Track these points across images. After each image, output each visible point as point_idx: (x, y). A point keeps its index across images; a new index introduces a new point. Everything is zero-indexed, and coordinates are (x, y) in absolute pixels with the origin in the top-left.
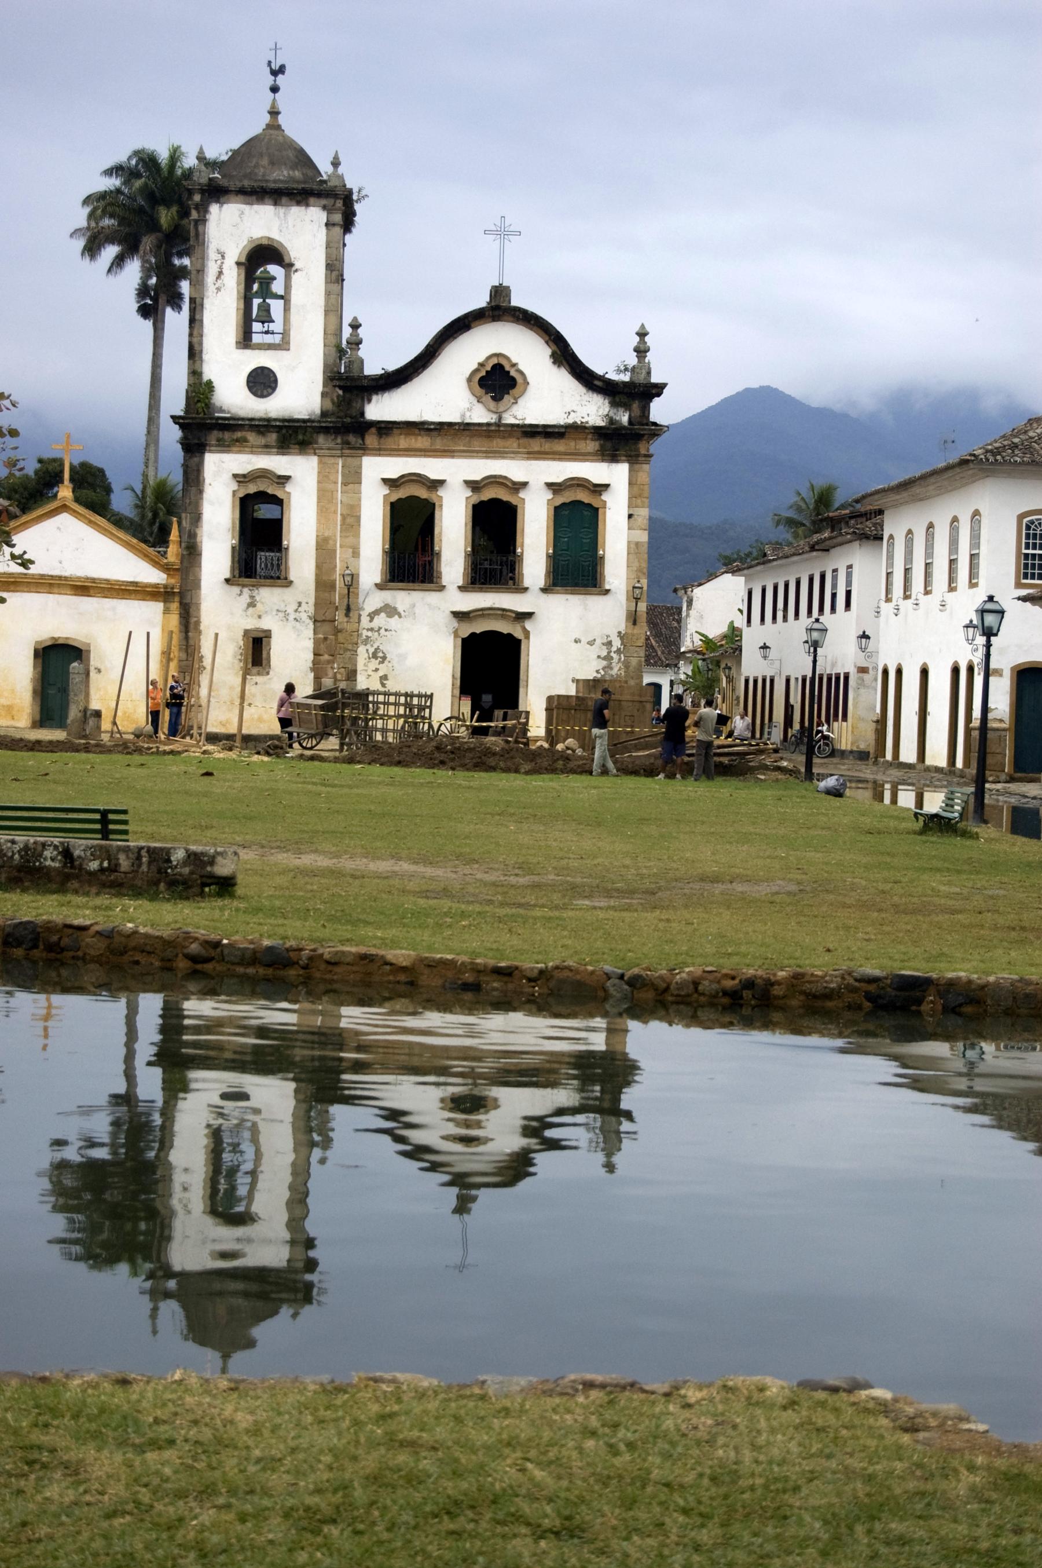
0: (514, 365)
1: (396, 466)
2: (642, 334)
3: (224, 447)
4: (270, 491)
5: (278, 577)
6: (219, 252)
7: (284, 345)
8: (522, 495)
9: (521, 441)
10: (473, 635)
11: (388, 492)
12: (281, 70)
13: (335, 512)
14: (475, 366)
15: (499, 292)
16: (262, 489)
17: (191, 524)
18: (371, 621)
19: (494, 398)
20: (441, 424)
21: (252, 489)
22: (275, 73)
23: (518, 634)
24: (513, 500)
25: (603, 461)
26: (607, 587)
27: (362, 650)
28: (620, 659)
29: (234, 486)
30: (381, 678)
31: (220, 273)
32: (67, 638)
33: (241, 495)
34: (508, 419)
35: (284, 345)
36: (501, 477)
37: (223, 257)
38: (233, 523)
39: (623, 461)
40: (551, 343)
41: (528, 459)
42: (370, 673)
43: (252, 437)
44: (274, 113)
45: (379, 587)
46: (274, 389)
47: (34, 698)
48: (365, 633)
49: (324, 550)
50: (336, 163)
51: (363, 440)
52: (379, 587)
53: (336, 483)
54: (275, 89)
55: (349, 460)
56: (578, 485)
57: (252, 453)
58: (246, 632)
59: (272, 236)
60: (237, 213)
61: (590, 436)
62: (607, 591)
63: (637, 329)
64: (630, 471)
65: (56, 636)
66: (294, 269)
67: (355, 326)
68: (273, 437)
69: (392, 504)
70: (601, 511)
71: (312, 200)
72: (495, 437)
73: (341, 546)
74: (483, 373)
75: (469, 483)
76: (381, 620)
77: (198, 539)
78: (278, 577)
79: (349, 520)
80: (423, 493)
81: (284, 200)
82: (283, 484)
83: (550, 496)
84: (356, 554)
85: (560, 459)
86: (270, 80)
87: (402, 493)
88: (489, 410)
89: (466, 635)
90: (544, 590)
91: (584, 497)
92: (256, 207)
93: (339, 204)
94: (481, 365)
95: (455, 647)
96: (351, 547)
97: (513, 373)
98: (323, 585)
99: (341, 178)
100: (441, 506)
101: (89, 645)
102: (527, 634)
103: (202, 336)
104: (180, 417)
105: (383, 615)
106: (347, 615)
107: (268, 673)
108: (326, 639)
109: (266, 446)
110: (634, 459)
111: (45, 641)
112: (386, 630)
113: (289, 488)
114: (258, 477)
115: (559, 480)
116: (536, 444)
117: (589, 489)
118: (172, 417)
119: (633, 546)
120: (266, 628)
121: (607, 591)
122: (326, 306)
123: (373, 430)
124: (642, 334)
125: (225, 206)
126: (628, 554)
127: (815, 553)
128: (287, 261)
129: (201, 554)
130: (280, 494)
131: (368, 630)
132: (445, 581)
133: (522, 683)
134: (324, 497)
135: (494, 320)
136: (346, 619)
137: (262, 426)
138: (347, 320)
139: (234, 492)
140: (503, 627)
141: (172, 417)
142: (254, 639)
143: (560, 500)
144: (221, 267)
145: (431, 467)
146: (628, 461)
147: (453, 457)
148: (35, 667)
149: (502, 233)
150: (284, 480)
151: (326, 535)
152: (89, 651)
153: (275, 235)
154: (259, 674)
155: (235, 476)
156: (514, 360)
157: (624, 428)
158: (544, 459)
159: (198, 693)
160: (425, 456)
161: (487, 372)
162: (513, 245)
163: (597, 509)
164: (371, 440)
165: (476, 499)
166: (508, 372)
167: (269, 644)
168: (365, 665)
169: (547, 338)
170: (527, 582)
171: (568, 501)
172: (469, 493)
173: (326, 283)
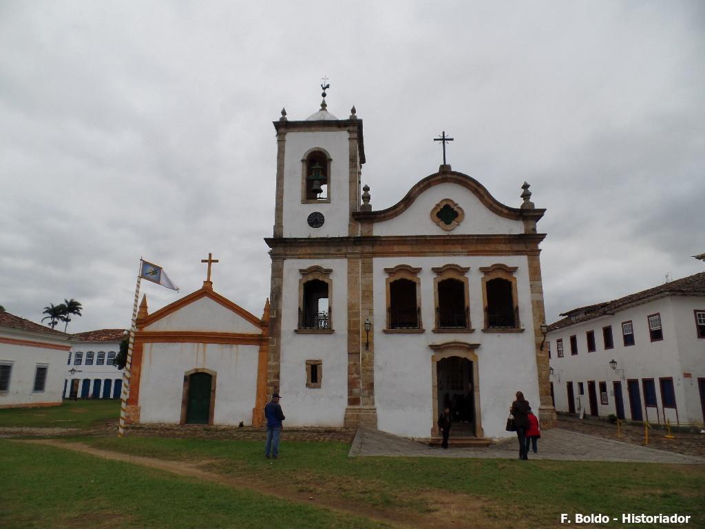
0: (456, 205)
1: (393, 262)
2: (526, 187)
4: (320, 279)
7: (328, 201)
8: (467, 275)
10: (443, 359)
11: (388, 277)
12: (328, 86)
13: (359, 289)
14: (434, 206)
15: (445, 169)
16: (316, 278)
21: (310, 278)
22: (324, 89)
23: (470, 357)
25: (512, 255)
26: (522, 328)
32: (204, 369)
33: (304, 281)
35: (328, 201)
36: (453, 265)
39: (524, 255)
41: (468, 255)
44: (324, 105)
45: (385, 332)
46: (322, 224)
47: (182, 406)
49: (352, 312)
50: (353, 111)
52: (385, 332)
53: (358, 273)
54: (324, 95)
55: (367, 260)
56: (500, 269)
57: (310, 258)
58: (307, 363)
59: (321, 146)
63: (522, 185)
67: (367, 189)
69: (391, 284)
70: (513, 284)
72: (447, 244)
73: (363, 309)
74: (439, 210)
77: (279, 308)
80: (409, 277)
82: (328, 274)
83: (483, 276)
84: (371, 311)
85: (487, 255)
86: (323, 91)
87: (397, 277)
88: (443, 229)
89: (439, 359)
90: (484, 331)
93: (356, 128)
94: (438, 205)
97: (456, 209)
98: (353, 332)
99: (356, 117)
101: (216, 373)
104: (269, 239)
108: (355, 364)
111: (191, 371)
114: (314, 271)
117: (506, 270)
118: (265, 239)
119: (535, 302)
122: (350, 179)
123: (378, 242)
124: (526, 187)
127: (606, 316)
128: (328, 157)
130: (326, 281)
132: (424, 327)
138: (362, 186)
139: (300, 281)
140: (461, 354)
141: (265, 239)
143: (489, 278)
145: (413, 262)
146: (526, 254)
147: (424, 256)
148: (184, 385)
149: (444, 139)
150: (329, 272)
151: (353, 302)
152: (215, 376)
154: (315, 387)
155: (301, 271)
156: (456, 202)
158: (478, 255)
160: (409, 256)
161: (441, 209)
162: (449, 144)
164: (377, 249)
165: (440, 279)
170: (473, 327)
171: (493, 278)
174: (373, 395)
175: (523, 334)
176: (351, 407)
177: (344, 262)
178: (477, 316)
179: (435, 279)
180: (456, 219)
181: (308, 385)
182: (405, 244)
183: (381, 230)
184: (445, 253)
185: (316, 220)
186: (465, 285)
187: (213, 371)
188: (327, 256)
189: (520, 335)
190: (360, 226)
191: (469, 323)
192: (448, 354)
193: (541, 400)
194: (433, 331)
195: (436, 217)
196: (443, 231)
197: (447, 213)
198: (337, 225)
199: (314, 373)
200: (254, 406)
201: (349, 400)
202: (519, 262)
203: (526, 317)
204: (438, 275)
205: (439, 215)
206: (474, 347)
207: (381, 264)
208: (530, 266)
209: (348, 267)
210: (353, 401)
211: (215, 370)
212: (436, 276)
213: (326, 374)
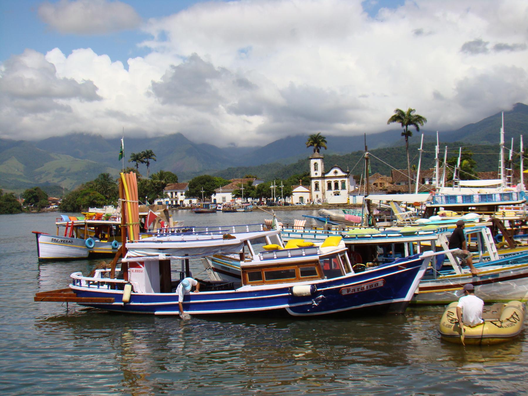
5: (319, 190)
34: (337, 175)
45: (327, 190)
49: (322, 187)
52: (327, 190)
78: (319, 190)
84: (325, 187)
90: (341, 190)
98: (322, 190)
110: (348, 178)
134: (322, 183)
150: (318, 182)
177: (321, 180)
183: (326, 176)
185: (316, 174)
188: (318, 179)
197: (336, 172)
198: (319, 175)
199: (317, 196)
202: (346, 179)
203: (347, 187)
206: (339, 192)
207: (326, 180)
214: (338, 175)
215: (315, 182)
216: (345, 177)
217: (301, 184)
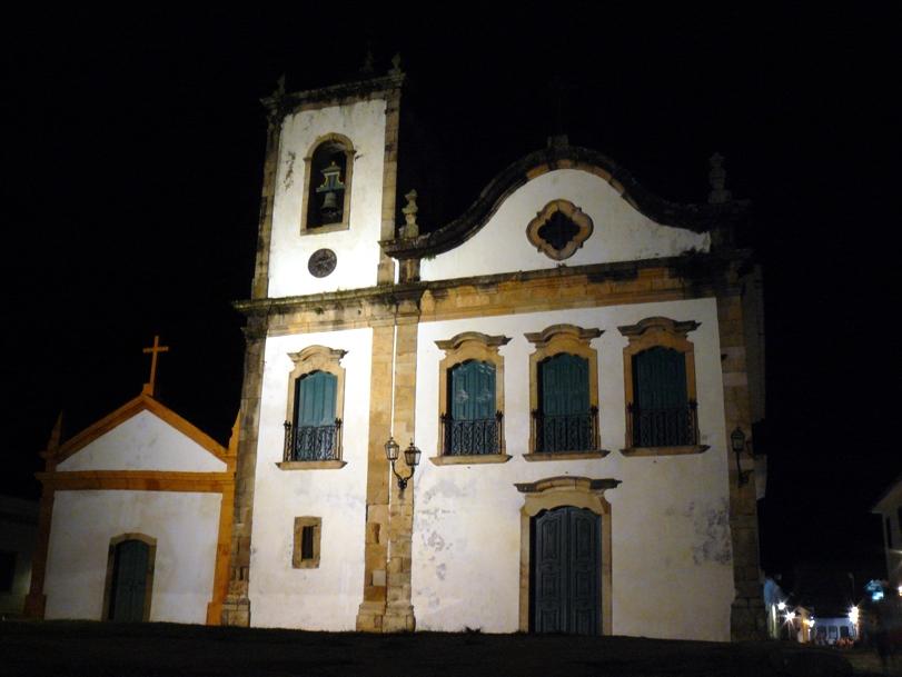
1: (448, 329)
3: (283, 330)
6: (290, 154)
9: (589, 288)
17: (249, 409)
18: (426, 503)
19: (556, 248)
20: (495, 276)
24: (583, 353)
25: (685, 298)
26: (703, 442)
27: (416, 537)
28: (725, 531)
29: (291, 366)
30: (438, 567)
31: (291, 171)
32: (138, 534)
34: (571, 262)
36: (565, 325)
37: (294, 158)
38: (288, 405)
40: (615, 183)
42: (426, 562)
43: (311, 316)
45: (436, 461)
48: (419, 517)
51: (418, 304)
53: (391, 353)
55: (404, 327)
58: (297, 520)
60: (308, 118)
61: (667, 272)
62: (705, 448)
64: (719, 306)
65: (128, 532)
66: (356, 155)
68: (330, 314)
71: (373, 94)
73: (395, 420)
74: (543, 223)
75: (532, 337)
76: (437, 501)
77: (255, 424)
79: (403, 391)
81: (348, 99)
84: (411, 427)
87: (459, 357)
90: (625, 452)
91: (664, 340)
92: (324, 110)
95: (522, 527)
96: (403, 421)
97: (575, 218)
100: (503, 367)
101: (155, 540)
102: (607, 507)
103: (270, 229)
105: (440, 495)
106: (401, 496)
107: (317, 566)
109: (322, 323)
111: (119, 537)
112: (444, 512)
113: (345, 362)
115: (633, 321)
116: (606, 287)
120: (316, 515)
121: (705, 448)
123: (427, 293)
125: (298, 115)
126: (725, 401)
129: (256, 440)
130: (334, 371)
131: (424, 512)
132: (508, 452)
133: (604, 569)
134: (379, 369)
135: (551, 169)
136: (399, 502)
137: (318, 304)
142: (305, 528)
144: (291, 167)
145: (489, 325)
146: (715, 294)
151: (380, 409)
152: (155, 547)
153: (339, 130)
154: (308, 567)
157: (707, 255)
159: (247, 590)
161: (547, 221)
163: (683, 355)
165: (541, 356)
166: (571, 219)
167: (319, 531)
168: (421, 553)
169: (609, 176)
170: (604, 446)
172: (532, 348)
173: (385, 162)
174: (410, 582)
175: (708, 451)
176: (369, 603)
177: (370, 331)
178: (612, 425)
179: (531, 356)
180: (575, 238)
181: (296, 565)
182: (477, 293)
184: (555, 305)
185: (322, 263)
186: (591, 365)
187: (150, 538)
188: (338, 323)
189: (700, 456)
190: (397, 262)
191: (597, 438)
192: (548, 501)
193: (736, 587)
194: (524, 456)
195: (539, 240)
196: (552, 261)
197: (557, 229)
199: (307, 540)
200: (211, 601)
201: (366, 593)
202: (703, 310)
204: (537, 347)
205: (542, 233)
206: (600, 485)
207: (432, 332)
208: (722, 319)
209: (374, 345)
210: (375, 591)
211: (154, 537)
212: (535, 350)
213: (327, 542)
214: (588, 254)
215: (300, 357)
216: (690, 274)
217: (148, 388)
